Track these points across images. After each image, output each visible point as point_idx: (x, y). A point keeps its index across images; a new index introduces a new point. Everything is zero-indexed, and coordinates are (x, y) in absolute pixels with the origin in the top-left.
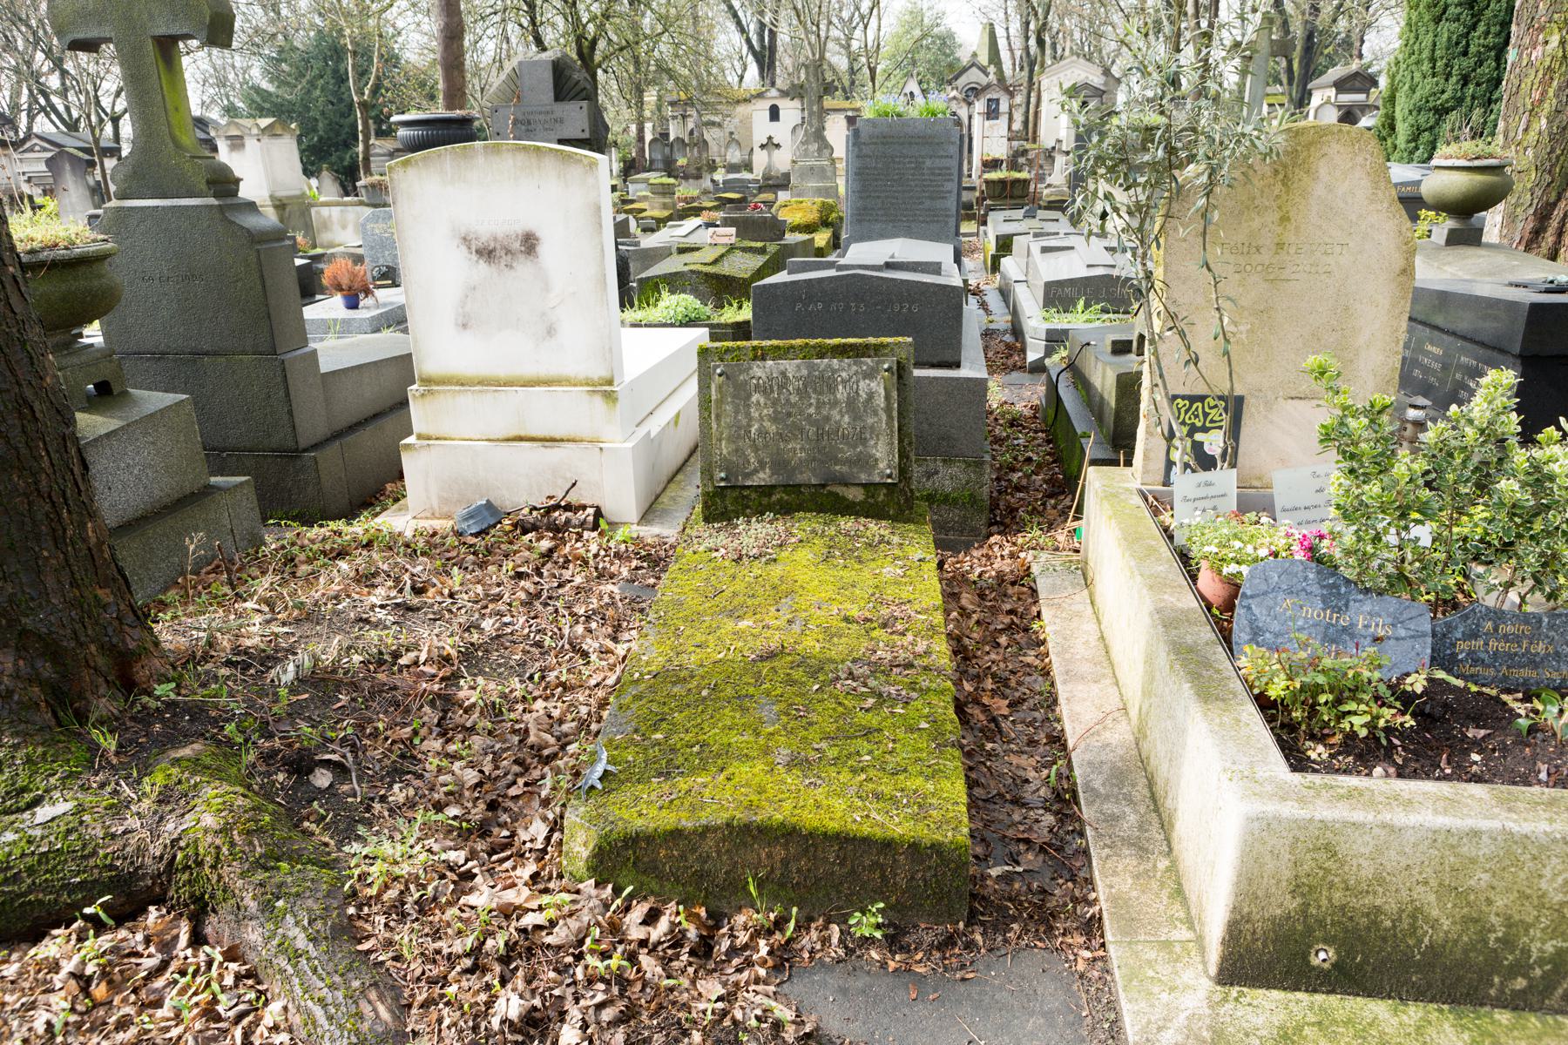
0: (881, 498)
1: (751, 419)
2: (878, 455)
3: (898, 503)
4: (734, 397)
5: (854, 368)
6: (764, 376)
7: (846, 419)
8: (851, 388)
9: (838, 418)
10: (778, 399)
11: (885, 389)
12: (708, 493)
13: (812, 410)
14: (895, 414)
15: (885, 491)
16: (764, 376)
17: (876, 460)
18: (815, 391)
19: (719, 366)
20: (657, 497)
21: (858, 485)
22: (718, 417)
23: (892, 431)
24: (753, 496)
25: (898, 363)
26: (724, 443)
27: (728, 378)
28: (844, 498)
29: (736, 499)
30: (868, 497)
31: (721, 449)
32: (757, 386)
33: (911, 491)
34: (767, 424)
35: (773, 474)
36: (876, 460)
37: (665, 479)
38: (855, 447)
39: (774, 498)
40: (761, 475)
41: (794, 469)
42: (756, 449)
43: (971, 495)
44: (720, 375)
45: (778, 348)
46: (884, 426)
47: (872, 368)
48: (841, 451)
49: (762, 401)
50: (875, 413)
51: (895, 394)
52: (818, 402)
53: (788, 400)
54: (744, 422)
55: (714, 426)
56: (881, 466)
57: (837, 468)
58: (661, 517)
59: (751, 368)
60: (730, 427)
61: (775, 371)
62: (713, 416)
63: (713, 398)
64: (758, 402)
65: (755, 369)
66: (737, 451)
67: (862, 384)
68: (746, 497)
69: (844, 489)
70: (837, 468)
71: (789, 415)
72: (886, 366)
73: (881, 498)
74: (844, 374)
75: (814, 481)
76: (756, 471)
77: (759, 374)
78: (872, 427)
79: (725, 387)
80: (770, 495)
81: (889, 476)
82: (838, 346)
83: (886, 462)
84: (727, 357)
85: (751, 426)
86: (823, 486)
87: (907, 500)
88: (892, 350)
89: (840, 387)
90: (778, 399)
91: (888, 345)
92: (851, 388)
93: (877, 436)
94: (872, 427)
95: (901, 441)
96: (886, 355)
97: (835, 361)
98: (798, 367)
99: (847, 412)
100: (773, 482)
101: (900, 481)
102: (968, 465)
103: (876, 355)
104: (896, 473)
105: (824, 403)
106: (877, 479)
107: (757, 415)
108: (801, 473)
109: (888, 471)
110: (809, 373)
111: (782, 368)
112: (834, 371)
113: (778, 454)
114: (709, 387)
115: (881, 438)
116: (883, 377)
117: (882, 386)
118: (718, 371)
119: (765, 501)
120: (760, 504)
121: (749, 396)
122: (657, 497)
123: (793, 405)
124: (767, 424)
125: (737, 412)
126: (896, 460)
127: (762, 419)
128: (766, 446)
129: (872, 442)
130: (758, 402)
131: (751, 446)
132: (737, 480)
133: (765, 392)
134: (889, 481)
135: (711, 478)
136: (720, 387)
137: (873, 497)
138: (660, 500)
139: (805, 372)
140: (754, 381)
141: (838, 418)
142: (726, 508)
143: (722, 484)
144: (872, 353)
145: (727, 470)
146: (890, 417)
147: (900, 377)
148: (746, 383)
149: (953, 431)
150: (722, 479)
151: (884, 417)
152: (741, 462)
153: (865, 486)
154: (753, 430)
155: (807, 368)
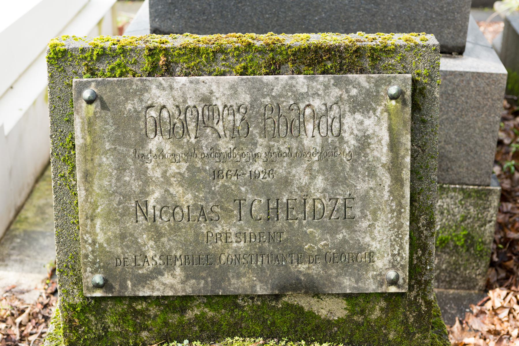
0: (376, 314)
1: (147, 182)
2: (375, 246)
3: (405, 322)
4: (117, 140)
5: (336, 92)
6: (170, 105)
7: (320, 182)
8: (330, 128)
9: (305, 180)
10: (197, 147)
11: (390, 129)
12: (73, 307)
13: (258, 167)
14: (406, 174)
15: (383, 304)
16: (170, 105)
17: (371, 254)
18: (264, 132)
19: (86, 85)
20: (19, 211)
21: (338, 295)
22: (87, 175)
23: (400, 205)
24: (153, 310)
25: (414, 82)
26: (98, 222)
27: (104, 106)
28: (311, 314)
29: (123, 316)
30: (353, 313)
31: (93, 233)
32: (158, 123)
33: (429, 304)
34: (176, 190)
35: (188, 277)
36: (371, 254)
37: (30, 180)
38: (334, 231)
39: (190, 314)
40: (167, 279)
41: (225, 270)
42: (158, 235)
43: (468, 236)
44: (90, 102)
45: (196, 52)
46: (386, 195)
47: (368, 93)
48: (309, 238)
49: (168, 148)
50: (371, 173)
51: (406, 140)
52: (269, 153)
53: (214, 149)
54: (136, 186)
55: (81, 193)
56: (380, 263)
57: (303, 267)
58: (21, 248)
59: (146, 89)
60: (110, 195)
61: (190, 94)
62: (79, 175)
63: (78, 142)
64: (161, 152)
65: (154, 90)
66: (123, 236)
67: (349, 121)
68: (141, 313)
69: (313, 301)
70: (303, 267)
71: (217, 174)
72: (393, 90)
73: (376, 314)
74: (317, 103)
75: (260, 290)
76: (157, 272)
77: (162, 101)
78: (365, 198)
79: (98, 124)
80: (183, 311)
81: (394, 282)
82: (306, 50)
83: (387, 258)
84: (105, 67)
85: (148, 194)
86: (277, 297)
87: (419, 317)
88: (403, 59)
89: (310, 126)
90: (197, 147)
91: (396, 50)
92: (330, 128)
93: (374, 213)
94: (365, 198)
95: (414, 219)
96: (392, 69)
97: (301, 78)
98: (233, 87)
99: (321, 170)
100: (189, 291)
101: (411, 288)
102: (467, 195)
103: (375, 69)
104: (404, 275)
105: (280, 154)
106: (371, 287)
107: (158, 174)
108: (239, 276)
109: (392, 274)
110: (254, 100)
111: (204, 90)
112: (299, 97)
113: (197, 242)
114: (70, 121)
115: (381, 216)
116: (387, 110)
117: (385, 125)
118: (87, 94)
119: (174, 318)
120: (166, 323)
121: (144, 139)
122: (18, 212)
123: (224, 157)
124: (176, 190)
125: (121, 168)
126: (406, 254)
127: (166, 180)
128: (175, 229)
129: (365, 224)
130: (161, 152)
131: (147, 229)
132: (124, 286)
133: (172, 132)
134: (393, 289)
135: (78, 281)
136: (90, 123)
137: (362, 312)
138: (23, 214)
139: (245, 98)
140: (153, 113)
141: (305, 180)
142: (105, 329)
143: (98, 294)
144: (367, 63)
145: (106, 269)
146: (397, 180)
147: (416, 108)
148: (136, 116)
149: (449, 148)
150: (97, 286)
151: (387, 180)
152: (130, 256)
153: (348, 297)
154: (151, 202)
155: (250, 90)
